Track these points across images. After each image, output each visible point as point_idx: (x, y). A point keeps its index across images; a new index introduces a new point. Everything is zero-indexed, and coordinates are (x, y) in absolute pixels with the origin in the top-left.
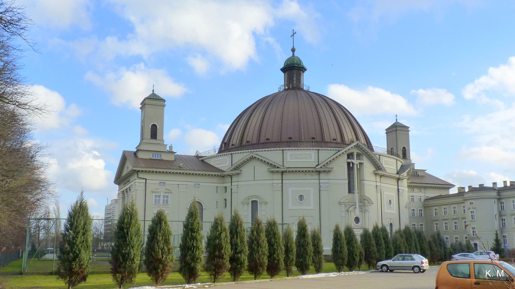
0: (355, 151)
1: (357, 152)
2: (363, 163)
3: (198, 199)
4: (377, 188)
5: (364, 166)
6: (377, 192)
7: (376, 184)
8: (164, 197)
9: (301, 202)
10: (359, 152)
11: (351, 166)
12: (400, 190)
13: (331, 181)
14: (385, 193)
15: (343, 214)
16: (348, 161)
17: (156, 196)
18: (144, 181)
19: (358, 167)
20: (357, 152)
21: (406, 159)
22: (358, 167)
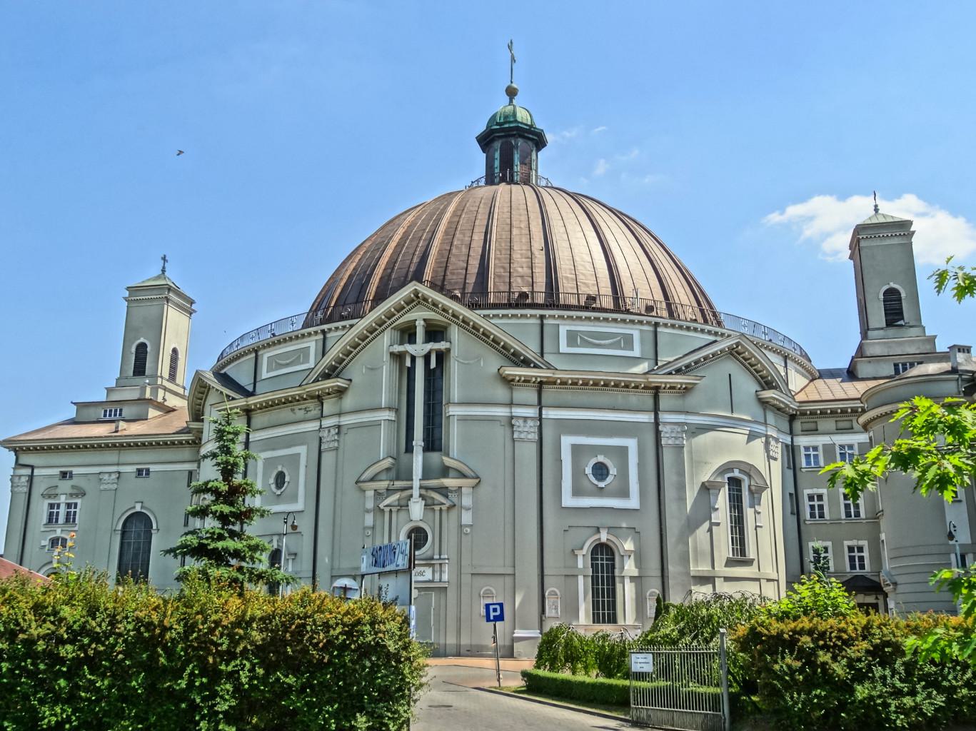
0: (419, 316)
1: (425, 320)
2: (448, 350)
3: (142, 508)
4: (512, 426)
5: (452, 359)
6: (514, 440)
7: (509, 414)
8: (69, 505)
9: (279, 492)
10: (430, 315)
11: (408, 364)
12: (661, 428)
13: (346, 420)
14: (567, 441)
15: (369, 519)
16: (391, 350)
17: (52, 506)
18: (28, 471)
19: (433, 365)
20: (425, 320)
21: (901, 326)
22: (433, 365)
